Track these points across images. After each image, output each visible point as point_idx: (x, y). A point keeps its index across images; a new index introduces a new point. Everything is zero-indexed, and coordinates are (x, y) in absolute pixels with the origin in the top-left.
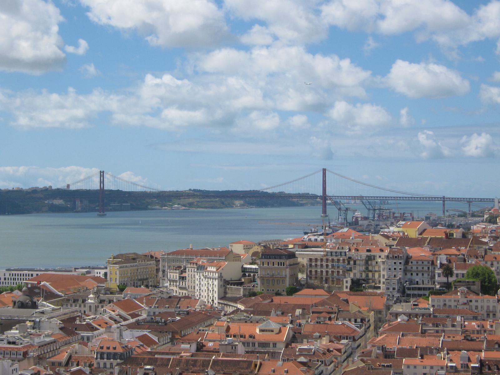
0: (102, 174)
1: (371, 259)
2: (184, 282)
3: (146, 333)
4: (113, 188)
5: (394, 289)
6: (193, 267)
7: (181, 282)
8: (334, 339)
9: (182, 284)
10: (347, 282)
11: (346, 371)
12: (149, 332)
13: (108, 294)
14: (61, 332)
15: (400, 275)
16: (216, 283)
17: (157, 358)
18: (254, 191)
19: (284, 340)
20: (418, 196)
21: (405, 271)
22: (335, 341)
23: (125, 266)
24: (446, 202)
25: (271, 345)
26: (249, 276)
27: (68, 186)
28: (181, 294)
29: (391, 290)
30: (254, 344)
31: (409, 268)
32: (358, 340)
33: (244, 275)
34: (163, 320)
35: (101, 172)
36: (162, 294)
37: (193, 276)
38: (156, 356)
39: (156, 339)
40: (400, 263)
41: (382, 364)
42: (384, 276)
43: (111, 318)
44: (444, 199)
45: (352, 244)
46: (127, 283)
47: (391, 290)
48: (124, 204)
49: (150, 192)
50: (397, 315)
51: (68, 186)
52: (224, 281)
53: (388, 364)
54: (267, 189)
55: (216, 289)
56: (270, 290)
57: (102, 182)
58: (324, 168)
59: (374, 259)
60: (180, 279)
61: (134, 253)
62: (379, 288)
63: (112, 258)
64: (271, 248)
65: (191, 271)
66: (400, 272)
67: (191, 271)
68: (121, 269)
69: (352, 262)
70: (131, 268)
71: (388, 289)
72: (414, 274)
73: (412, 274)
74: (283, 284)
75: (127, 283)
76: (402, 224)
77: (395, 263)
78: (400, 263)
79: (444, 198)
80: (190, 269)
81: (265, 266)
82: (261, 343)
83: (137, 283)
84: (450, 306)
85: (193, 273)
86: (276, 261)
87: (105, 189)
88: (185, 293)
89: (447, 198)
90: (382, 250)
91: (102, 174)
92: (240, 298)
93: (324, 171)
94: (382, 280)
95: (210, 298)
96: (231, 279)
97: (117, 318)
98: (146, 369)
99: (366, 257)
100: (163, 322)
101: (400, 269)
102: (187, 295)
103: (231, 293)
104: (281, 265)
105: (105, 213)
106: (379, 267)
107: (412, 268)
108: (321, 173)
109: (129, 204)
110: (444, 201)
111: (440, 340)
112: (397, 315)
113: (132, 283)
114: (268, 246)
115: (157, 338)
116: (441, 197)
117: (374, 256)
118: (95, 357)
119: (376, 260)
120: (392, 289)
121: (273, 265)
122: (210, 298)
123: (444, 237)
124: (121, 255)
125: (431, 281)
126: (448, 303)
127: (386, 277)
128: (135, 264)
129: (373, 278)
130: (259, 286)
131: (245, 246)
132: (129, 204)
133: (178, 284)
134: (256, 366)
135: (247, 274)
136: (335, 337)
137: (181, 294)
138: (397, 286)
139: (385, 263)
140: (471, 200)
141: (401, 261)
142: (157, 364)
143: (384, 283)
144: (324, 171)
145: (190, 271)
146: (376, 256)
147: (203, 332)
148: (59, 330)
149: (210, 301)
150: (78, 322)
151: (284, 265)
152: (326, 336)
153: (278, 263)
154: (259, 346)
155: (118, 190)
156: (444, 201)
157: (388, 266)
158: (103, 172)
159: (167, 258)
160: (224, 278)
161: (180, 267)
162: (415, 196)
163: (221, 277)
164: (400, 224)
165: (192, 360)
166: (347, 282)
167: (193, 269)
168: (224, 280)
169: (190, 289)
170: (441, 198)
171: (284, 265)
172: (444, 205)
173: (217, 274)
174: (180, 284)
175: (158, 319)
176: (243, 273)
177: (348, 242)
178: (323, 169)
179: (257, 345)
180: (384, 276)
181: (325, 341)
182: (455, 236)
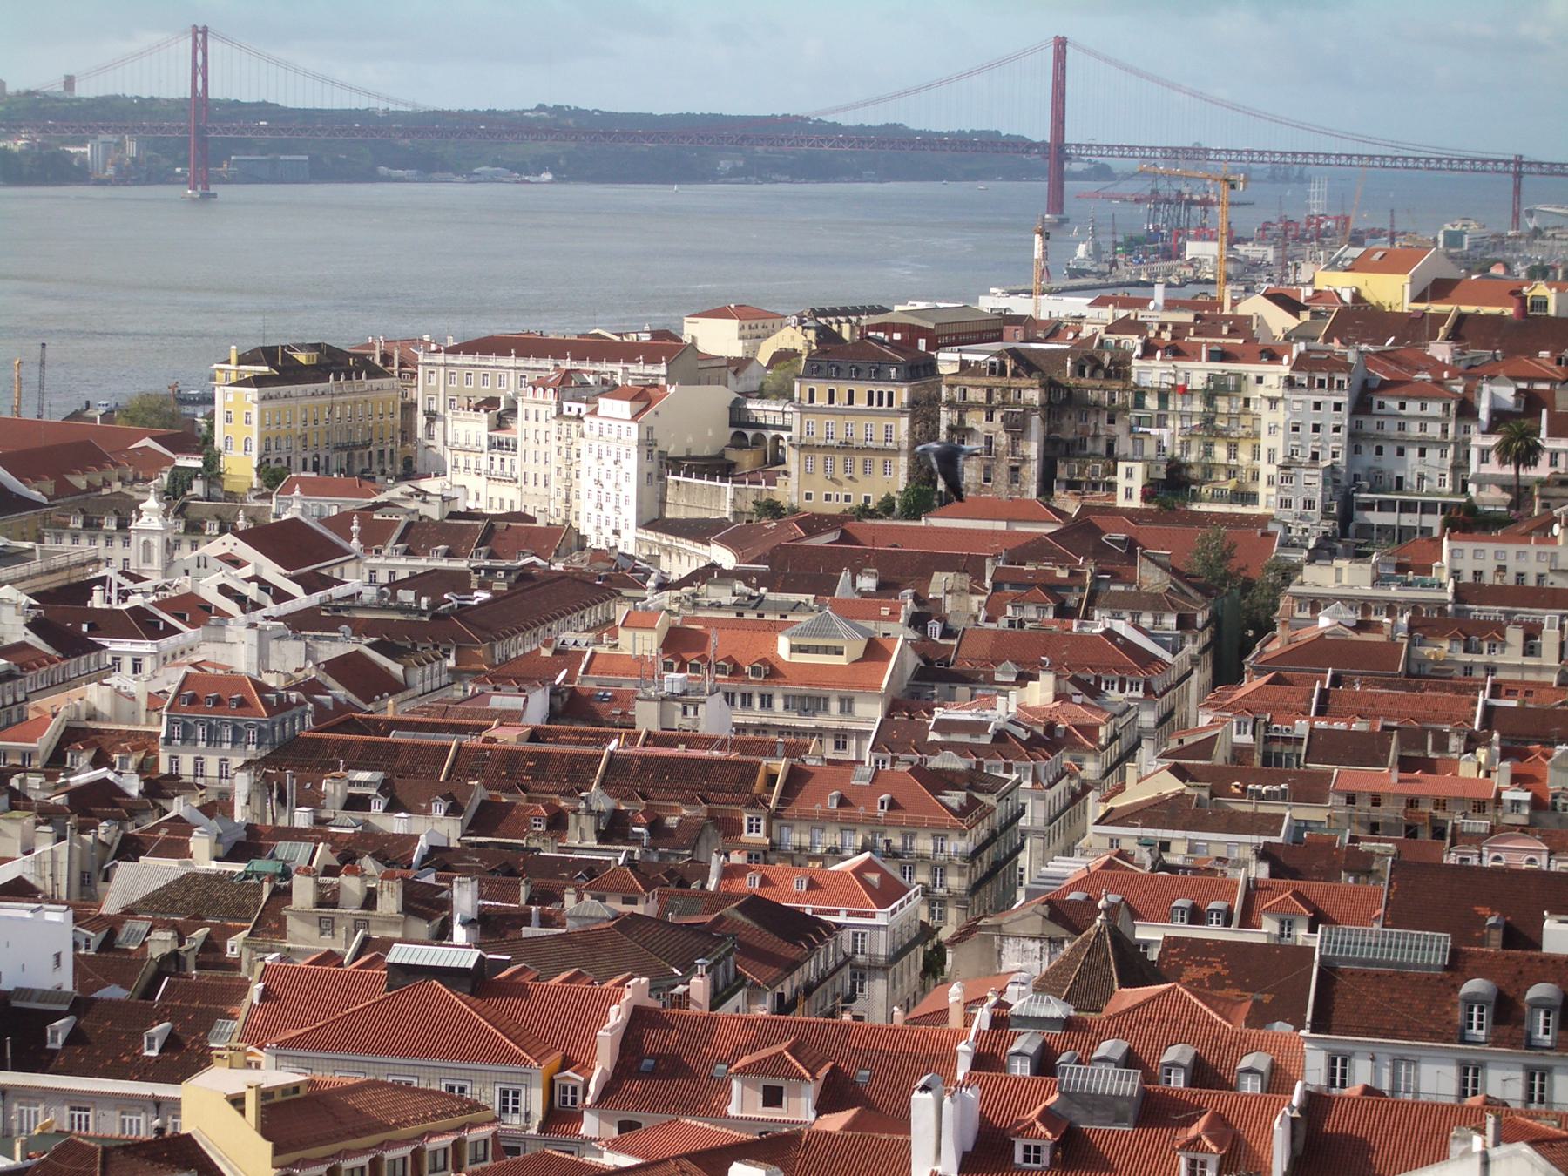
0: (200, 37)
1: (1226, 386)
2: (507, 458)
3: (352, 648)
4: (248, 94)
5: (1309, 504)
6: (543, 403)
7: (497, 457)
8: (1071, 689)
9: (502, 467)
10: (1129, 475)
11: (1112, 809)
12: (369, 646)
13: (219, 500)
14: (33, 639)
15: (1334, 447)
16: (631, 465)
17: (397, 745)
18: (788, 121)
19: (884, 685)
20: (1417, 154)
21: (1356, 438)
22: (1075, 694)
23: (282, 394)
24: (1526, 178)
25: (834, 706)
26: (759, 441)
27: (69, 82)
28: (496, 503)
29: (1297, 507)
30: (767, 702)
31: (1370, 424)
32: (1162, 694)
33: (739, 441)
34: (424, 600)
35: (195, 30)
36: (424, 501)
37: (541, 437)
38: (394, 736)
39: (396, 669)
40: (1337, 407)
41: (1250, 787)
42: (1271, 454)
43: (224, 590)
44: (1519, 169)
45: (1156, 327)
46: (289, 459)
47: (1297, 507)
48: (282, 157)
49: (387, 111)
50: (1316, 604)
51: (69, 82)
52: (660, 457)
53: (1275, 788)
54: (837, 110)
55: (630, 489)
56: (834, 498)
57: (200, 70)
59: (1238, 388)
60: (492, 447)
61: (317, 347)
62: (1251, 498)
63: (234, 359)
64: (846, 335)
65: (537, 419)
66: (1337, 440)
67: (537, 419)
68: (268, 404)
69: (1151, 403)
70: (305, 401)
71: (1284, 503)
72: (1390, 450)
73: (1379, 451)
74: (888, 476)
75: (289, 459)
76: (1353, 259)
77: (1317, 406)
78: (1337, 407)
79: (1519, 162)
80: (532, 409)
81: (817, 403)
82: (794, 697)
83: (327, 459)
84: (1520, 576)
85: (542, 425)
86: (861, 389)
87: (214, 94)
88: (512, 502)
89: (1530, 164)
90: (1273, 356)
91: (200, 37)
92: (720, 524)
93: (1061, 45)
94: (1267, 469)
95: (607, 523)
96: (688, 450)
97: (252, 591)
98: (352, 783)
99: (1209, 380)
100: (424, 606)
101: (1337, 429)
102: (517, 509)
103: (685, 502)
104: (880, 404)
105: (213, 189)
106: (1257, 418)
107: (1381, 426)
108: (1050, 51)
109: (306, 158)
110: (1518, 175)
111: (1475, 704)
112: (1316, 604)
113: (309, 456)
114: (835, 327)
115: (402, 667)
116: (1507, 158)
117: (1241, 377)
118: (163, 735)
119: (1244, 394)
120: (1301, 504)
121: (851, 402)
122: (607, 523)
123: (1509, 311)
124: (264, 349)
125: (1454, 480)
126: (1513, 566)
127: (1280, 460)
128: (321, 387)
129: (1233, 462)
130: (794, 479)
131: (747, 327)
132: (306, 158)
133: (484, 465)
134: (772, 778)
135: (750, 433)
136: (1075, 681)
137: (496, 503)
138: (1320, 494)
139: (1281, 405)
141: (1339, 400)
142: (399, 764)
143: (1270, 482)
144: (1061, 45)
145: (532, 416)
146: (1245, 378)
147: (575, 648)
148: (26, 630)
149: (607, 532)
150: (97, 601)
151: (890, 404)
152: (1043, 675)
153: (871, 394)
154: (786, 707)
155: (265, 103)
156: (1518, 175)
157: (1288, 415)
158: (205, 31)
159: (446, 365)
160: (662, 447)
161: (491, 403)
163: (648, 444)
164: (1344, 256)
165: (533, 756)
166: (1129, 475)
167: (542, 409)
168: (662, 454)
169: (530, 487)
170: (1507, 162)
171: (890, 404)
173: (634, 426)
174: (492, 466)
175: (407, 596)
176: (733, 430)
177: (1139, 319)
179: (778, 703)
180: (1271, 454)
181: (1040, 693)
182: (1552, 310)
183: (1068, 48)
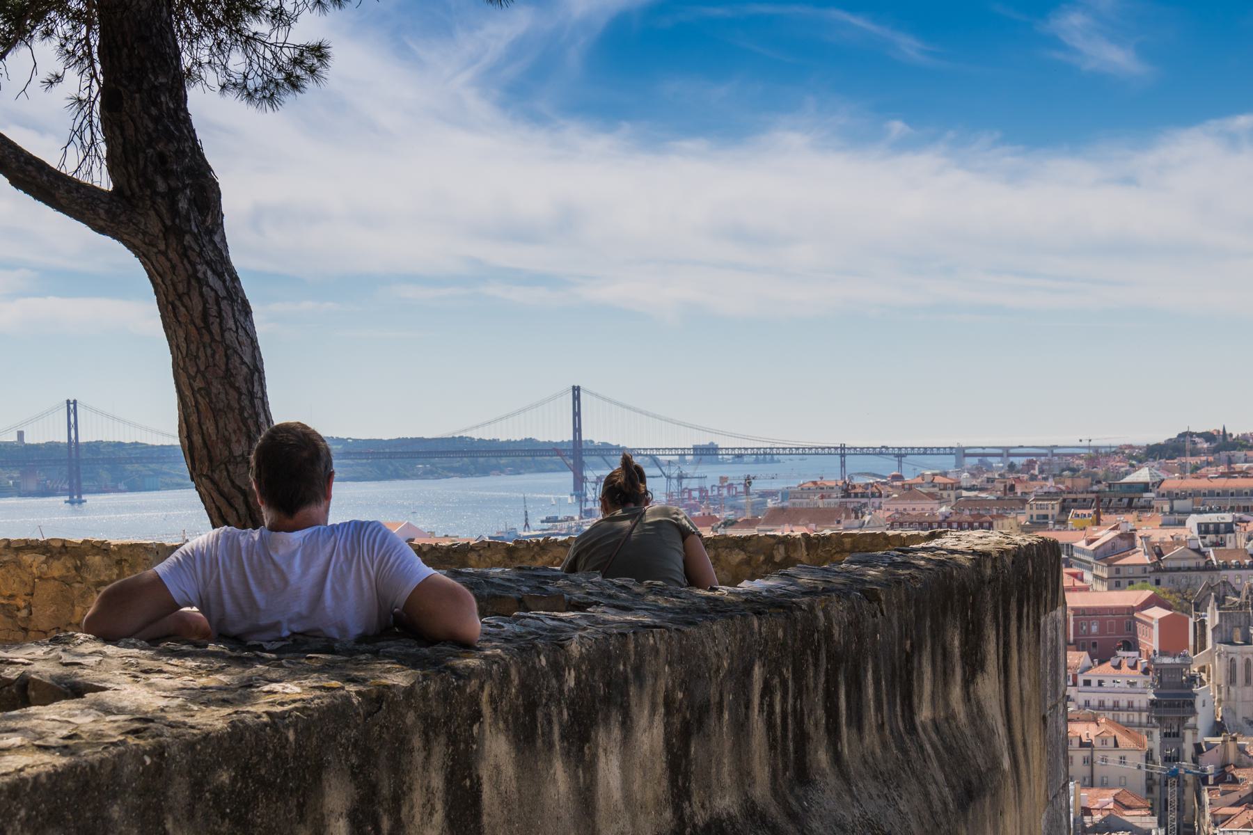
0: (72, 406)
27: (21, 434)
35: (68, 402)
44: (843, 452)
51: (21, 434)
57: (72, 426)
58: (576, 385)
79: (843, 448)
87: (80, 440)
91: (72, 406)
93: (576, 390)
110: (843, 455)
140: (903, 451)
144: (576, 390)
156: (843, 455)
158: (75, 402)
162: (777, 446)
170: (836, 448)
172: (843, 464)
178: (574, 387)
183: (582, 393)
